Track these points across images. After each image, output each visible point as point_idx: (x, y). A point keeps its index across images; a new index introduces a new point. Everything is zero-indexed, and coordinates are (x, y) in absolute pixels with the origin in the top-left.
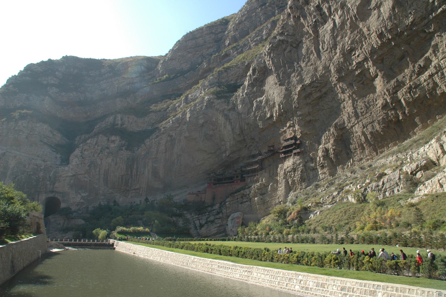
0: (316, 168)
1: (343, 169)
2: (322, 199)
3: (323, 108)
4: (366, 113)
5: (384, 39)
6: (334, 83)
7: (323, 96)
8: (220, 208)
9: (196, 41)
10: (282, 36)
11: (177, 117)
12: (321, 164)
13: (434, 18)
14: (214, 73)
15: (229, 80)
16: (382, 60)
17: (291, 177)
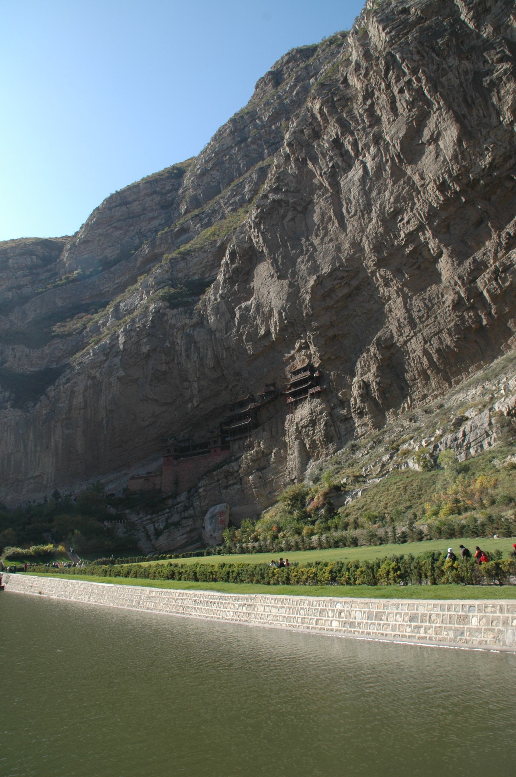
0: (350, 416)
1: (396, 414)
2: (363, 469)
3: (355, 313)
4: (428, 317)
5: (448, 193)
7: (354, 292)
8: (188, 498)
9: (128, 208)
10: (278, 194)
11: (102, 343)
12: (358, 409)
14: (163, 262)
15: (190, 274)
16: (448, 227)
17: (308, 435)
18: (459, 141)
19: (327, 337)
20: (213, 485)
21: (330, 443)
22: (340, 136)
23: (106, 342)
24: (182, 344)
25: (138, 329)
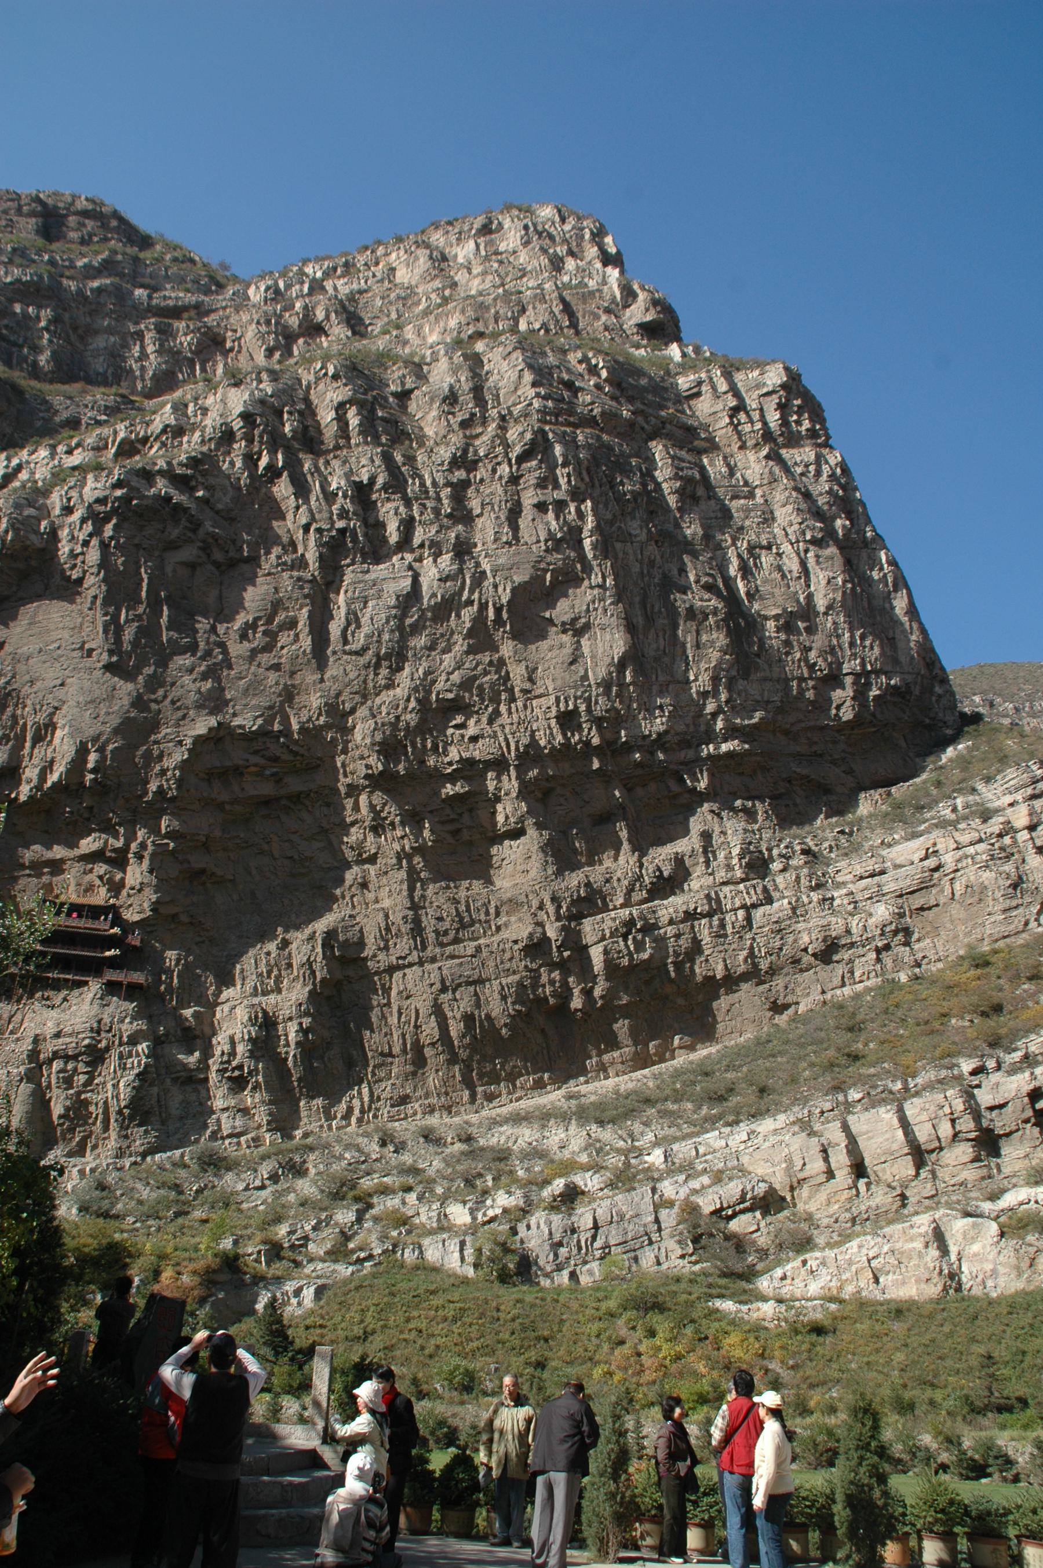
3: (266, 847)
4: (456, 941)
5: (573, 735)
6: (349, 780)
7: (284, 802)
10: (182, 492)
12: (233, 1069)
13: (710, 756)
16: (547, 793)
17: (68, 1082)
18: (621, 666)
21: (140, 1125)
22: (377, 487)
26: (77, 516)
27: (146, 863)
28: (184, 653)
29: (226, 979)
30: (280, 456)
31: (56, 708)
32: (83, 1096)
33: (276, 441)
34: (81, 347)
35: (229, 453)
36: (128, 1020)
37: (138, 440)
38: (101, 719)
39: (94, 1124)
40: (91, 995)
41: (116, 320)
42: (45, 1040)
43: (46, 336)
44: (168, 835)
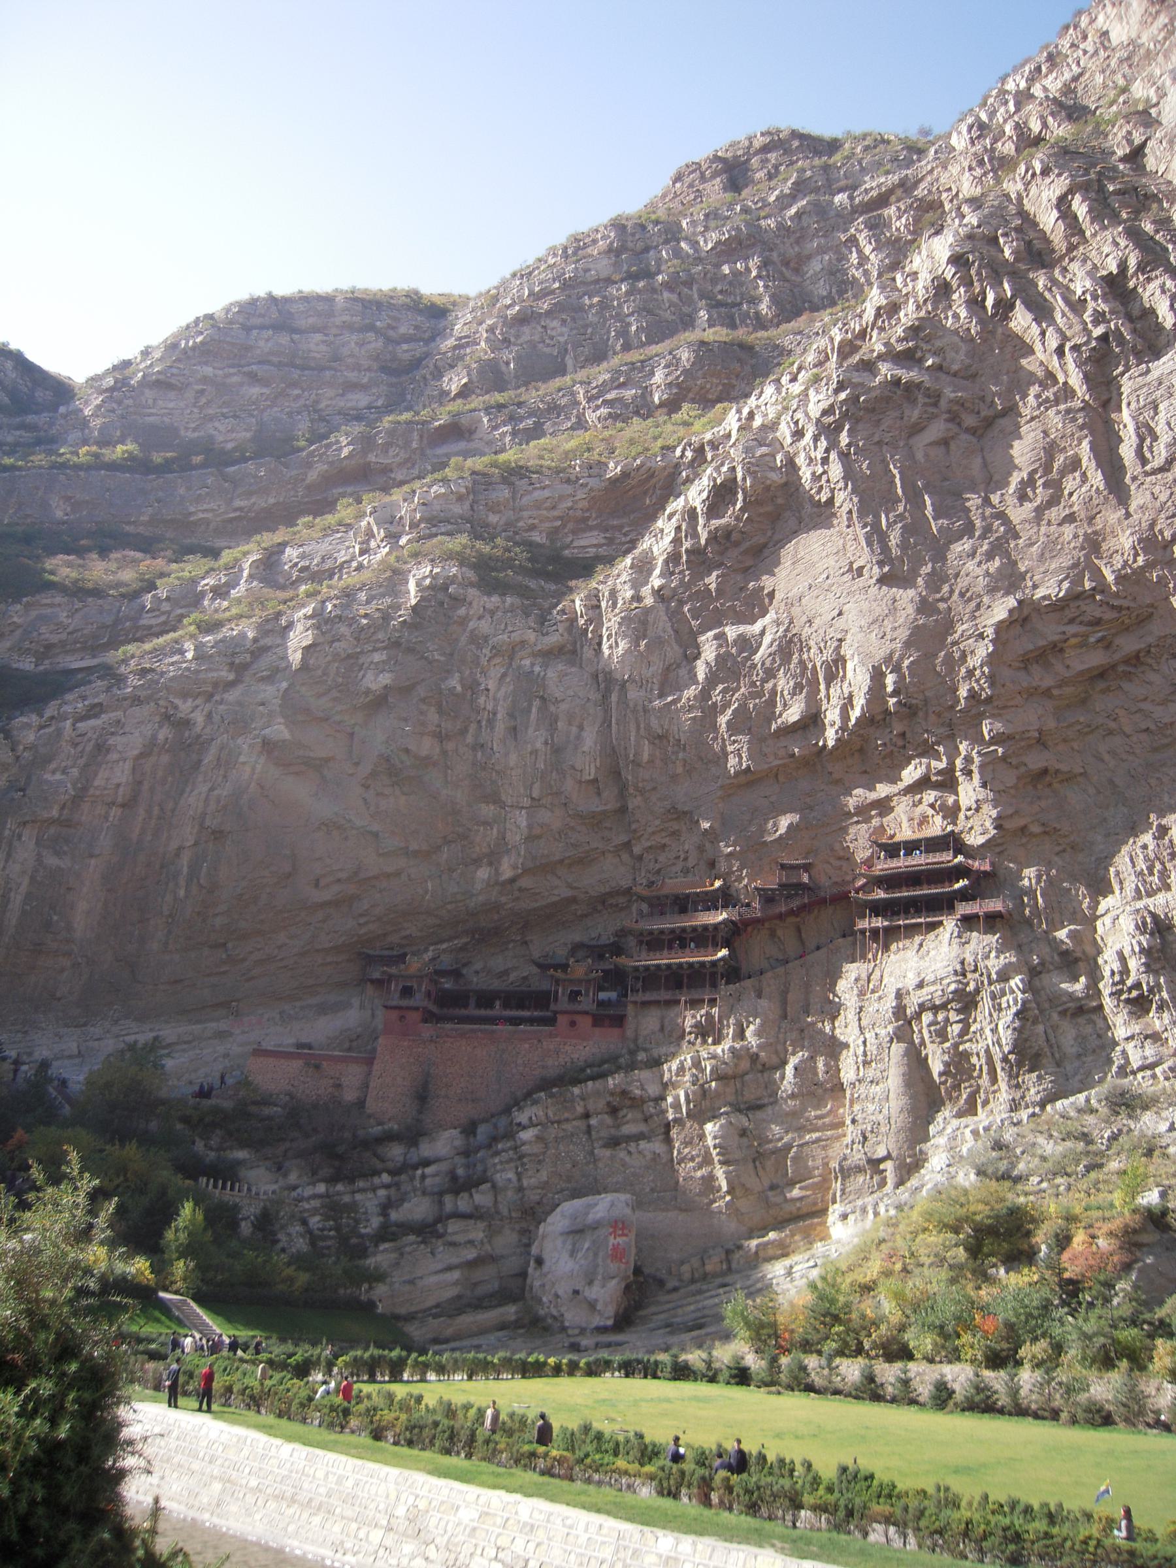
3: (1113, 725)
7: (1121, 668)
8: (466, 1153)
9: (292, 341)
10: (909, 369)
11: (225, 632)
12: (1130, 990)
14: (448, 472)
15: (521, 524)
17: (942, 1035)
19: (1023, 769)
20: (568, 1127)
21: (1031, 1071)
22: (1131, 271)
23: (242, 635)
24: (501, 694)
25: (365, 621)
26: (808, 436)
27: (976, 777)
28: (961, 538)
29: (1101, 888)
30: (1006, 286)
31: (840, 640)
32: (961, 1048)
33: (996, 271)
34: (799, 279)
35: (950, 307)
36: (993, 954)
37: (856, 337)
38: (888, 637)
39: (980, 1077)
40: (948, 935)
41: (824, 236)
42: (908, 993)
43: (761, 283)
44: (994, 741)
